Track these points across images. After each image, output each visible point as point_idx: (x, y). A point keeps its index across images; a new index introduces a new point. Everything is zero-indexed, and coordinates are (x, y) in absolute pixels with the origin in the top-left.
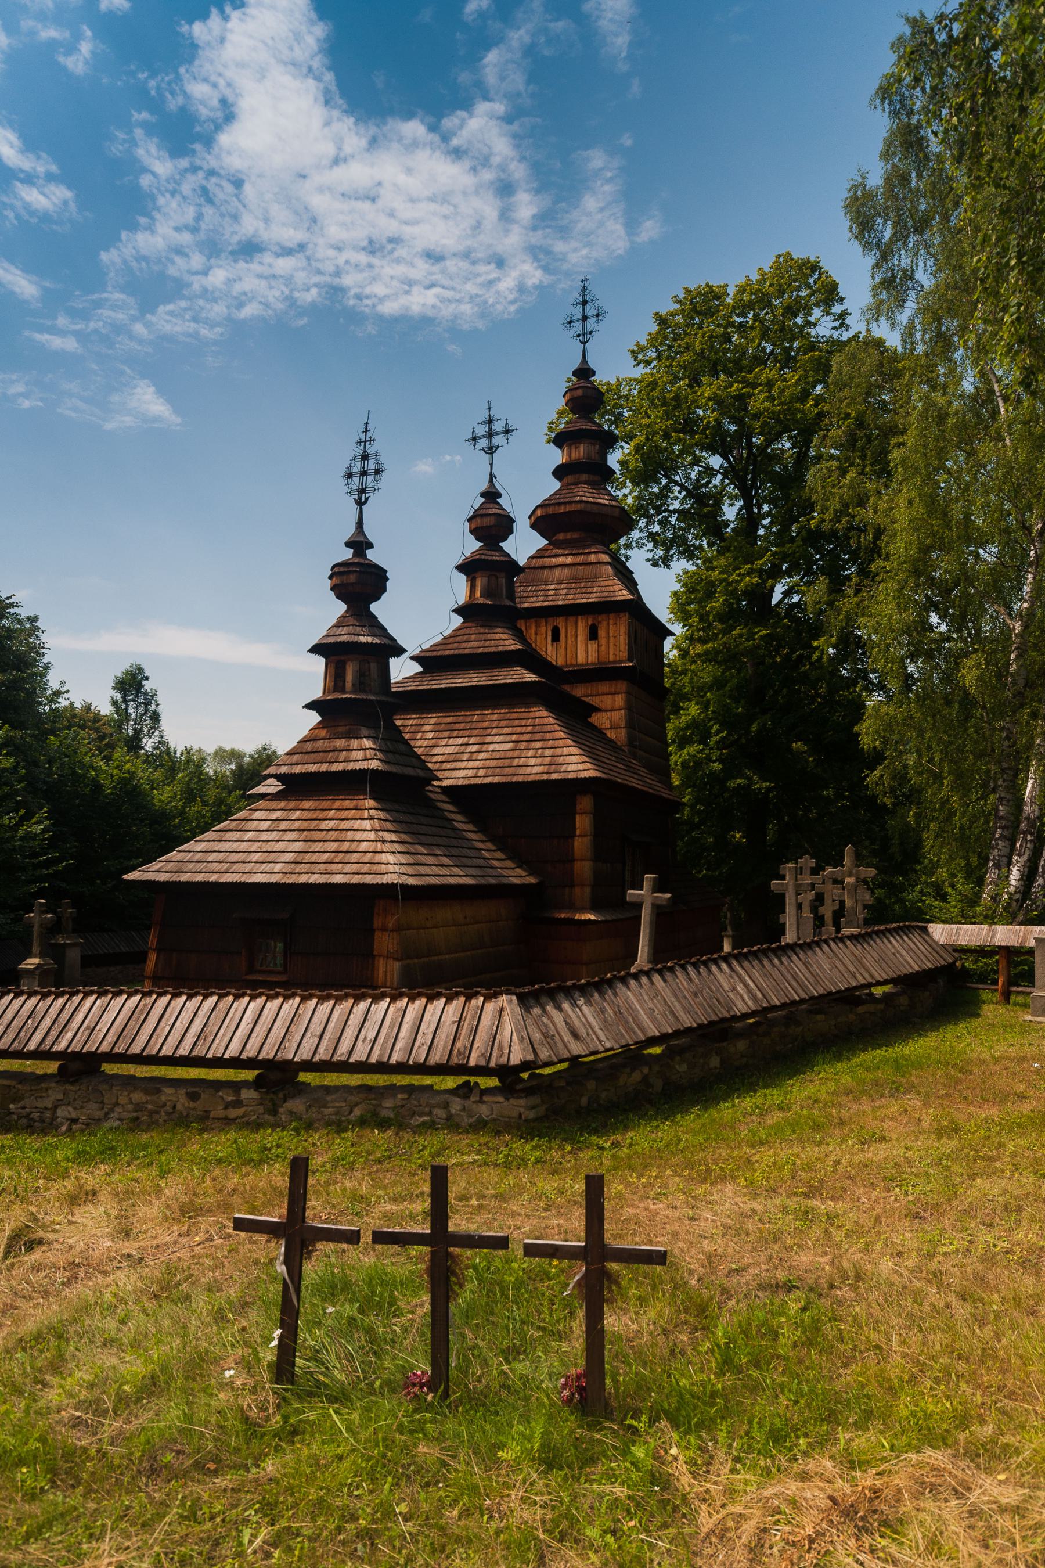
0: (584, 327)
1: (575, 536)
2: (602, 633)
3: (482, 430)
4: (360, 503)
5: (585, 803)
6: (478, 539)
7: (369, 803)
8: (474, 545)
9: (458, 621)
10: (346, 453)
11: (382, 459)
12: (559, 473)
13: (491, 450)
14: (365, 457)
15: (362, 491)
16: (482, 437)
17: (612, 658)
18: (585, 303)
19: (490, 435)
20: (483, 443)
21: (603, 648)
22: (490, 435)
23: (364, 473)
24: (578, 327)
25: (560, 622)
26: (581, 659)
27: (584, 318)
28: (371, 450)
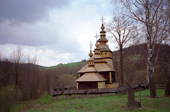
1: (103, 43)
5: (110, 73)
10: (89, 44)
13: (97, 38)
19: (97, 36)
20: (96, 37)
22: (97, 36)
24: (102, 20)
25: (102, 52)
26: (105, 56)
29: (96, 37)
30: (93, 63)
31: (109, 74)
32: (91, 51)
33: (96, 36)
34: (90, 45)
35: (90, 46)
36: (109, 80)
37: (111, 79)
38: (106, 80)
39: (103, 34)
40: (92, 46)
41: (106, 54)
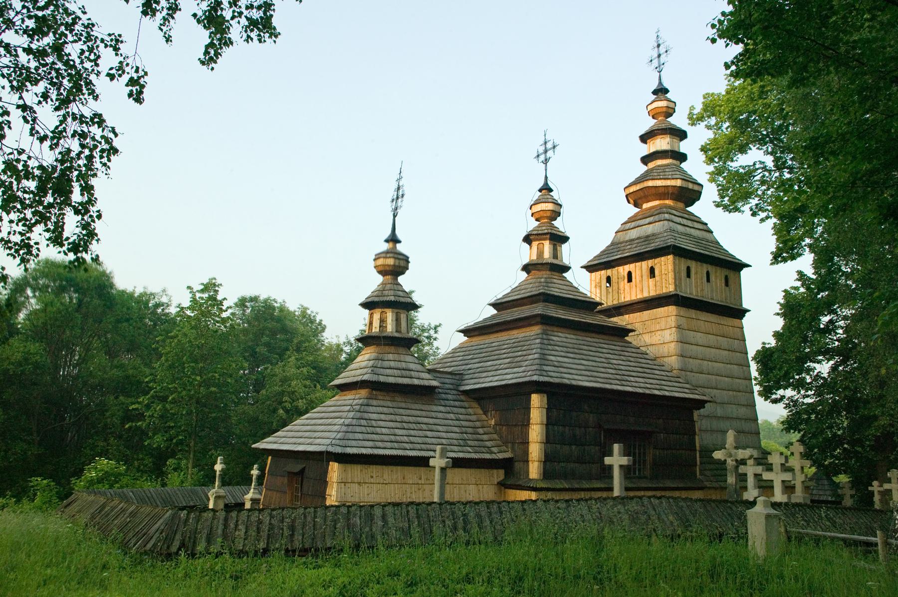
0: (659, 61)
2: (657, 272)
3: (542, 149)
4: (395, 216)
5: (536, 401)
8: (533, 224)
9: (524, 275)
12: (645, 160)
13: (546, 161)
15: (396, 209)
18: (659, 46)
19: (546, 151)
20: (542, 158)
22: (546, 151)
27: (659, 56)
30: (382, 321)
31: (528, 409)
37: (535, 450)
38: (508, 455)
39: (662, 143)
41: (652, 271)
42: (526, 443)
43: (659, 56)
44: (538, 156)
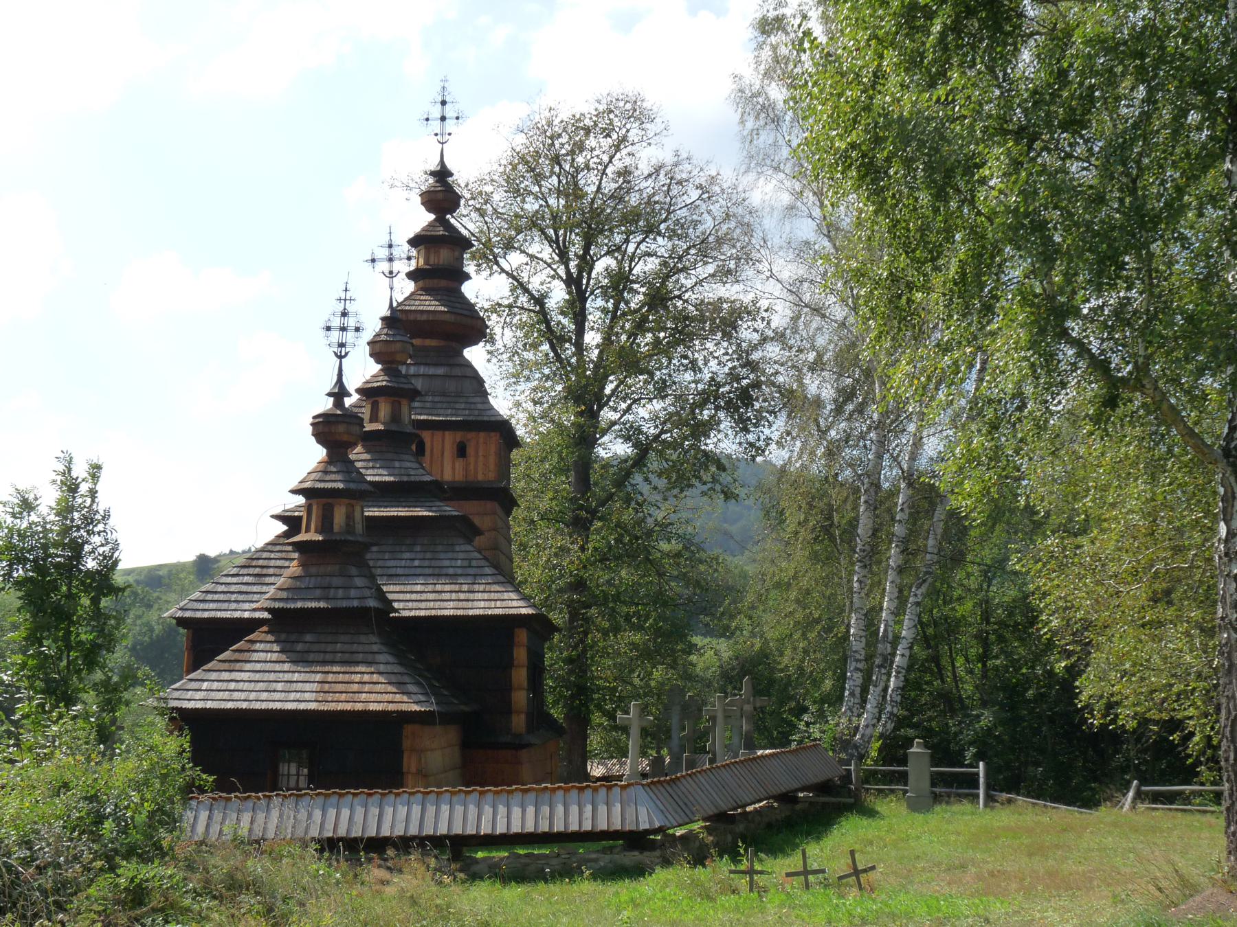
0: (442, 128)
2: (470, 450)
6: (377, 362)
7: (373, 639)
10: (328, 309)
11: (362, 319)
13: (391, 274)
14: (344, 314)
16: (382, 260)
17: (480, 477)
18: (444, 103)
20: (385, 266)
21: (472, 467)
22: (391, 260)
23: (343, 329)
24: (436, 125)
26: (448, 476)
27: (443, 119)
28: (350, 307)
29: (385, 266)
32: (339, 393)
33: (384, 253)
34: (337, 322)
35: (335, 336)
36: (507, 709)
39: (444, 256)
40: (350, 336)
42: (506, 689)
43: (443, 119)
44: (373, 261)
